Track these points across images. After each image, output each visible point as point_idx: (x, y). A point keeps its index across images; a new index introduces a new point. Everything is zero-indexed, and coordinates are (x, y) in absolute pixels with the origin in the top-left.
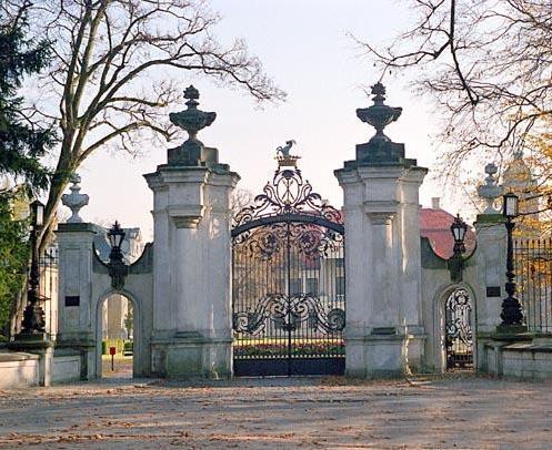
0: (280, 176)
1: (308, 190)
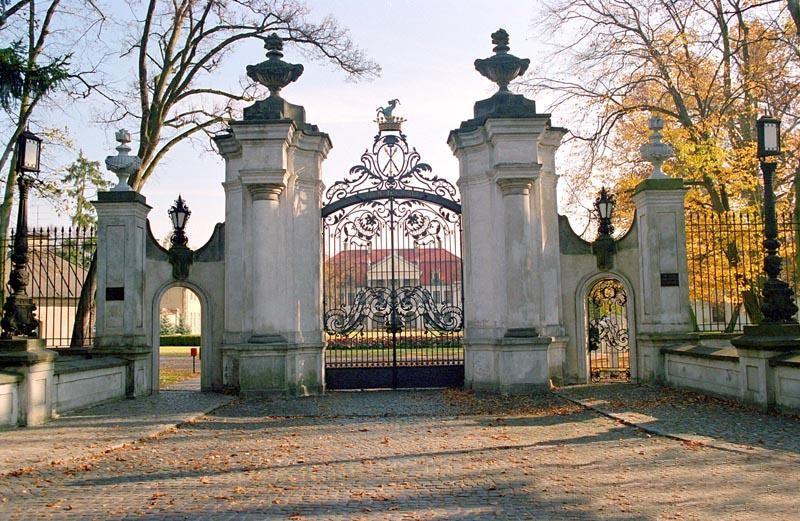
0: (380, 143)
1: (415, 160)
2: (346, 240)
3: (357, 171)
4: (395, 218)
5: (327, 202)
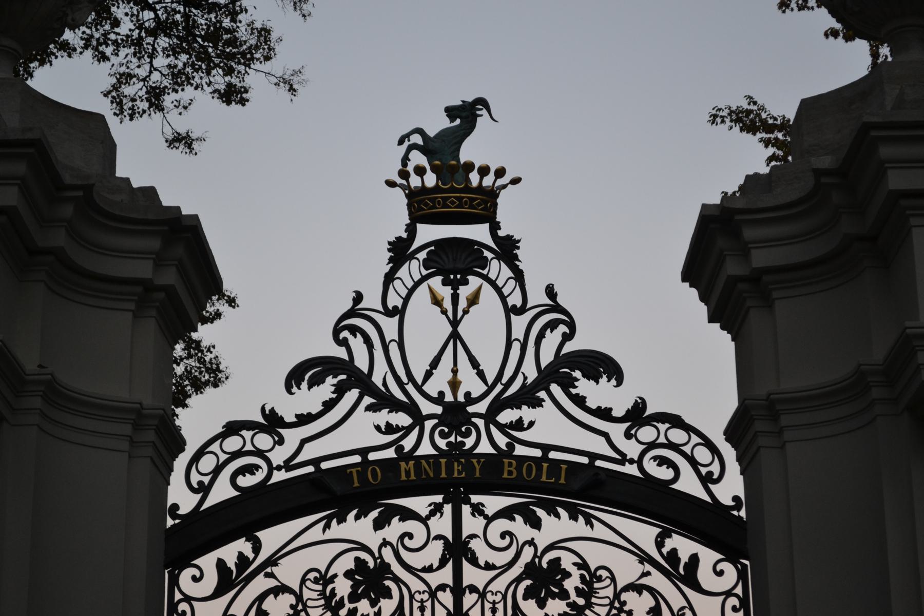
0: (412, 270)
1: (552, 340)
3: (315, 382)
4: (472, 575)
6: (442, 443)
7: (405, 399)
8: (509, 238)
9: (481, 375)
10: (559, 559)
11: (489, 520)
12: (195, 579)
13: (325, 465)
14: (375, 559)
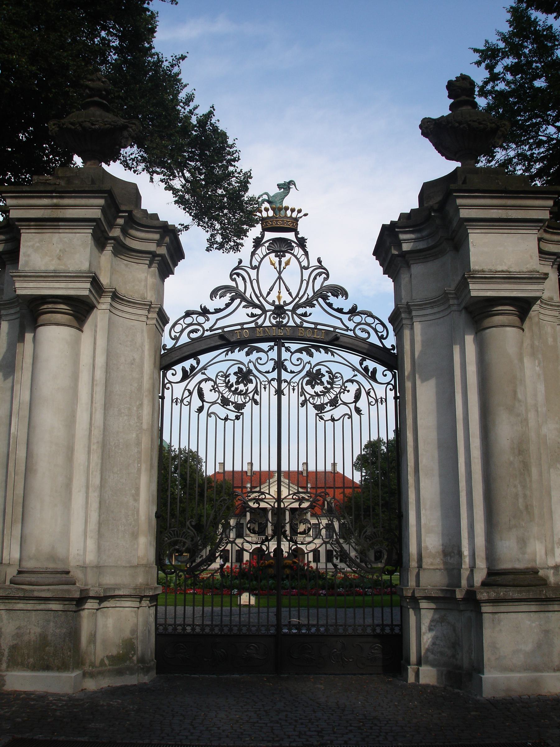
0: (262, 251)
1: (320, 280)
2: (200, 410)
4: (285, 376)
5: (170, 344)
6: (274, 322)
7: (258, 303)
8: (303, 238)
9: (290, 294)
10: (320, 369)
11: (292, 353)
12: (173, 374)
13: (226, 330)
14: (246, 368)
